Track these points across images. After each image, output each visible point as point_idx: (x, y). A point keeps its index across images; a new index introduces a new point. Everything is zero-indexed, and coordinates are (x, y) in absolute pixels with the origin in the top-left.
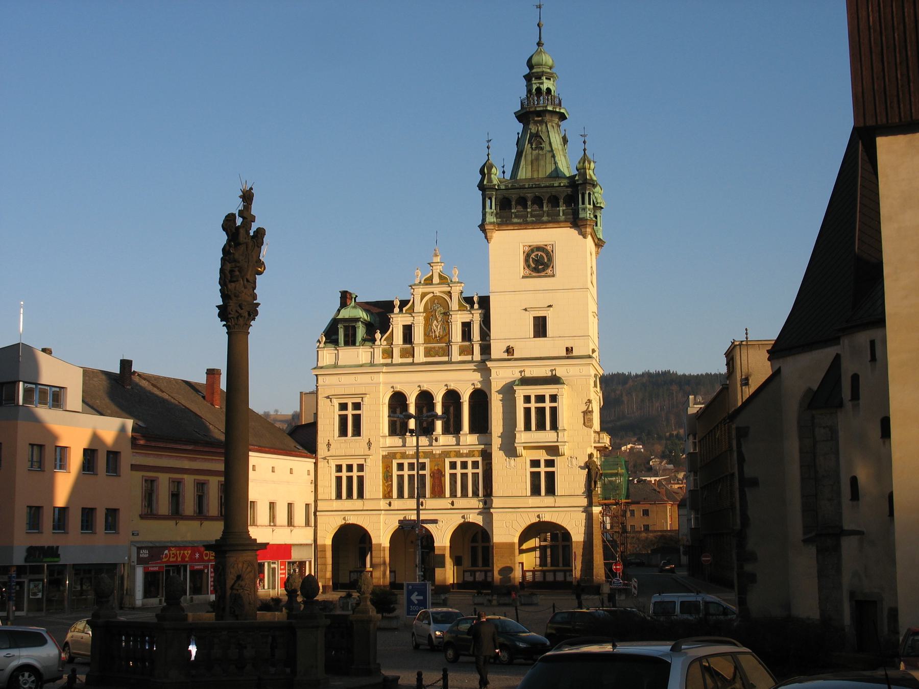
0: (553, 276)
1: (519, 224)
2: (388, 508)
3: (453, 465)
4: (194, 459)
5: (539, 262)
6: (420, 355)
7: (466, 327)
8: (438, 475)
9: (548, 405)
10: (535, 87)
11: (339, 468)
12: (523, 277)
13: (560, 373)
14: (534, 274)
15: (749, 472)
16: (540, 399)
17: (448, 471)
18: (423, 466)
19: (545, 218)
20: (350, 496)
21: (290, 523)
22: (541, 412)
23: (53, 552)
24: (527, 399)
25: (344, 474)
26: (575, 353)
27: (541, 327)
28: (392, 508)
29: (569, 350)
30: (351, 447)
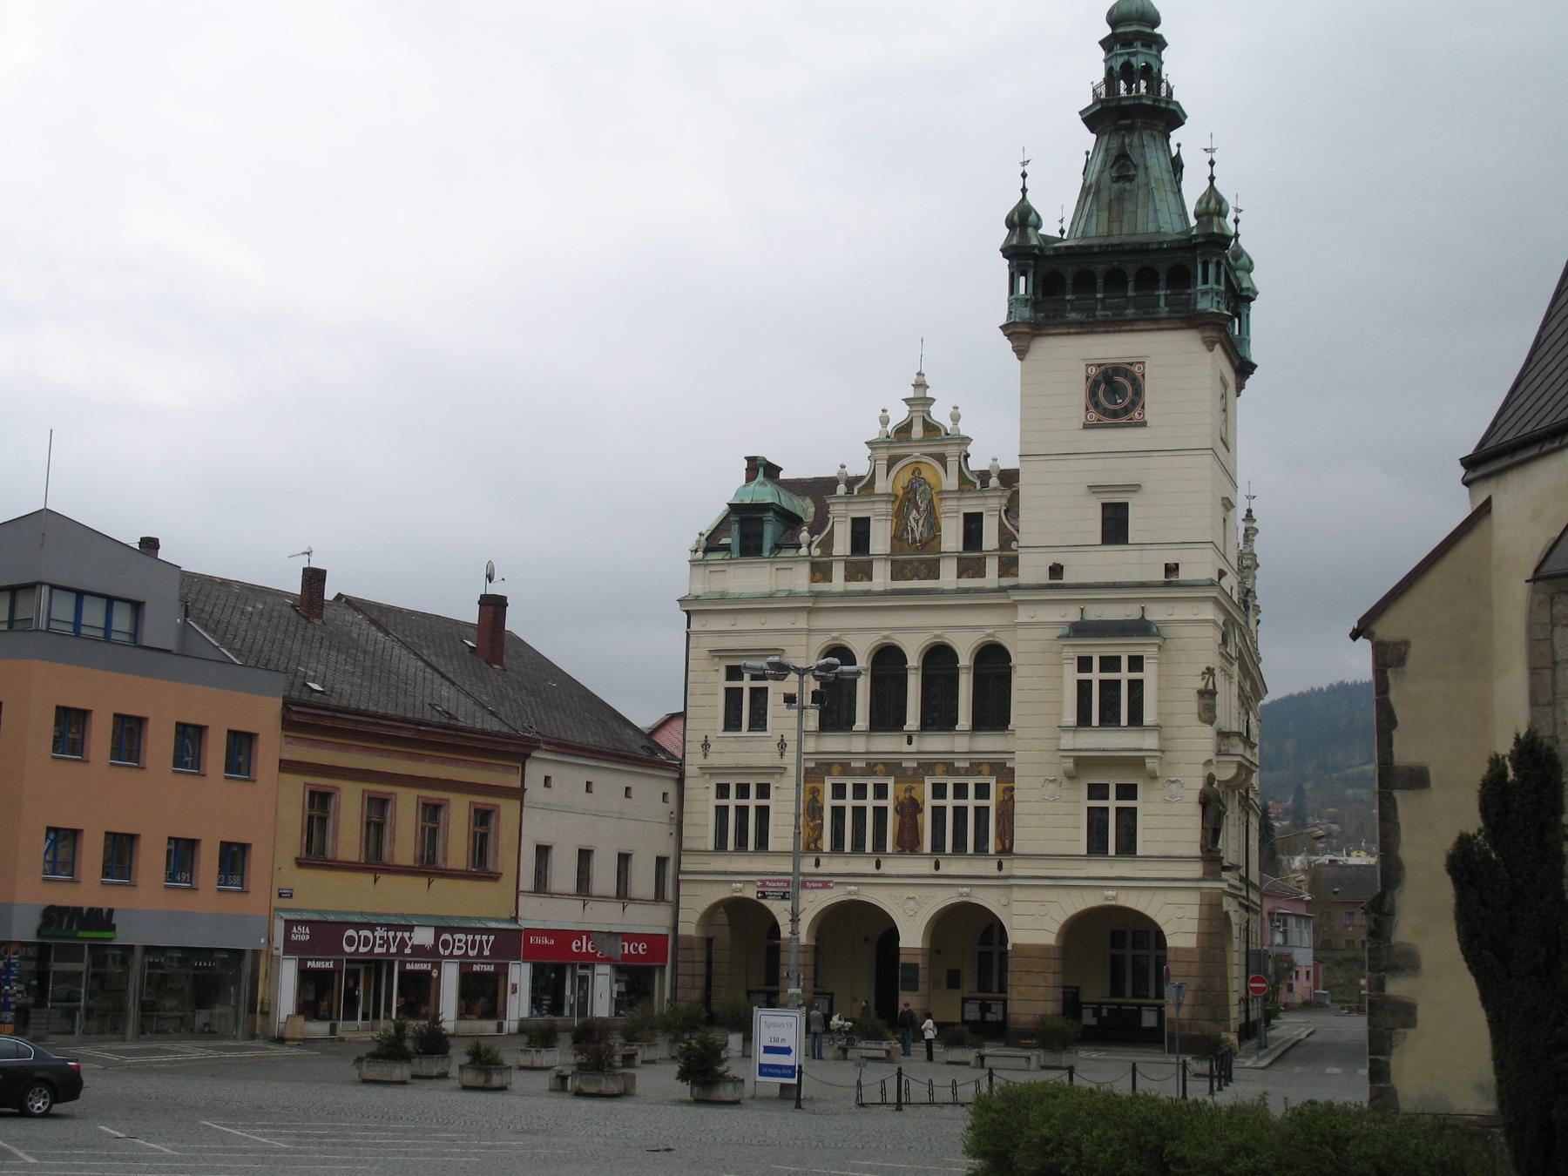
0: (1144, 424)
1: (1080, 324)
3: (939, 791)
4: (421, 758)
5: (1115, 396)
6: (881, 577)
7: (973, 524)
8: (909, 809)
9: (1124, 675)
10: (1121, 60)
11: (723, 791)
13: (1156, 613)
14: (1107, 420)
15: (1405, 752)
16: (1110, 663)
17: (929, 802)
18: (881, 791)
19: (1130, 312)
20: (741, 843)
21: (622, 893)
22: (1110, 688)
23: (101, 919)
24: (1084, 664)
25: (732, 802)
26: (1184, 575)
27: (1115, 525)
29: (1171, 569)
30: (748, 751)
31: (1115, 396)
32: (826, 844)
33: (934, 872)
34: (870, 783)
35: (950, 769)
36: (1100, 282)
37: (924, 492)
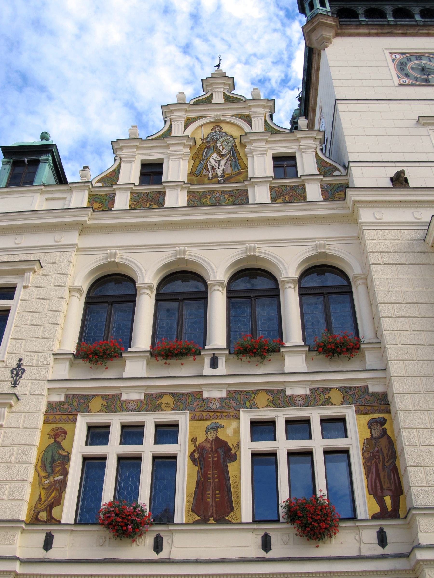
2: (39, 553)
3: (262, 429)
8: (214, 458)
18: (167, 432)
28: (53, 554)
32: (68, 510)
33: (262, 554)
34: (150, 421)
35: (279, 398)
37: (226, 141)
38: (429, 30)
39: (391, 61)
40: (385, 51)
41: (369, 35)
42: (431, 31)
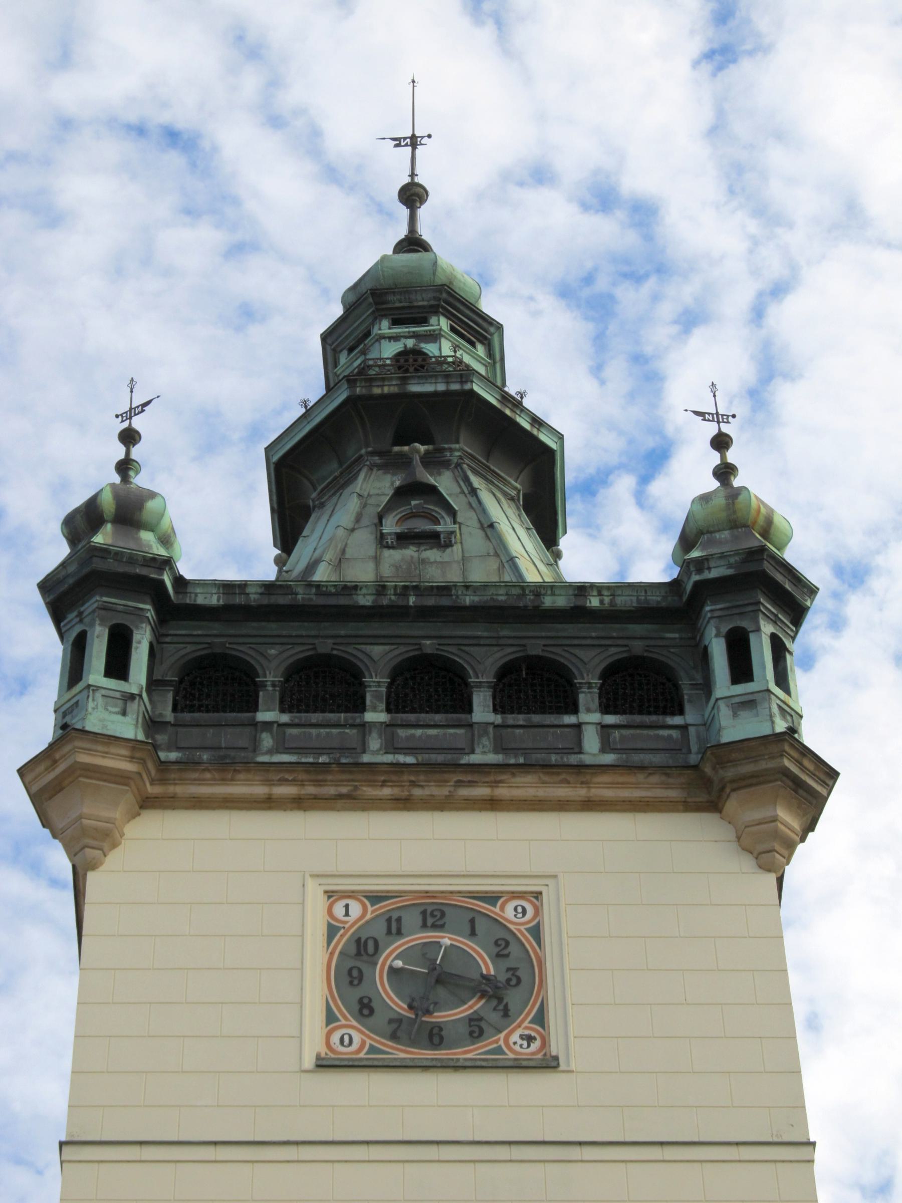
10: (389, 350)
12: (323, 1065)
14: (401, 1053)
31: (441, 992)
36: (376, 683)
38: (495, 784)
39: (321, 931)
40: (311, 884)
41: (268, 803)
42: (502, 792)
